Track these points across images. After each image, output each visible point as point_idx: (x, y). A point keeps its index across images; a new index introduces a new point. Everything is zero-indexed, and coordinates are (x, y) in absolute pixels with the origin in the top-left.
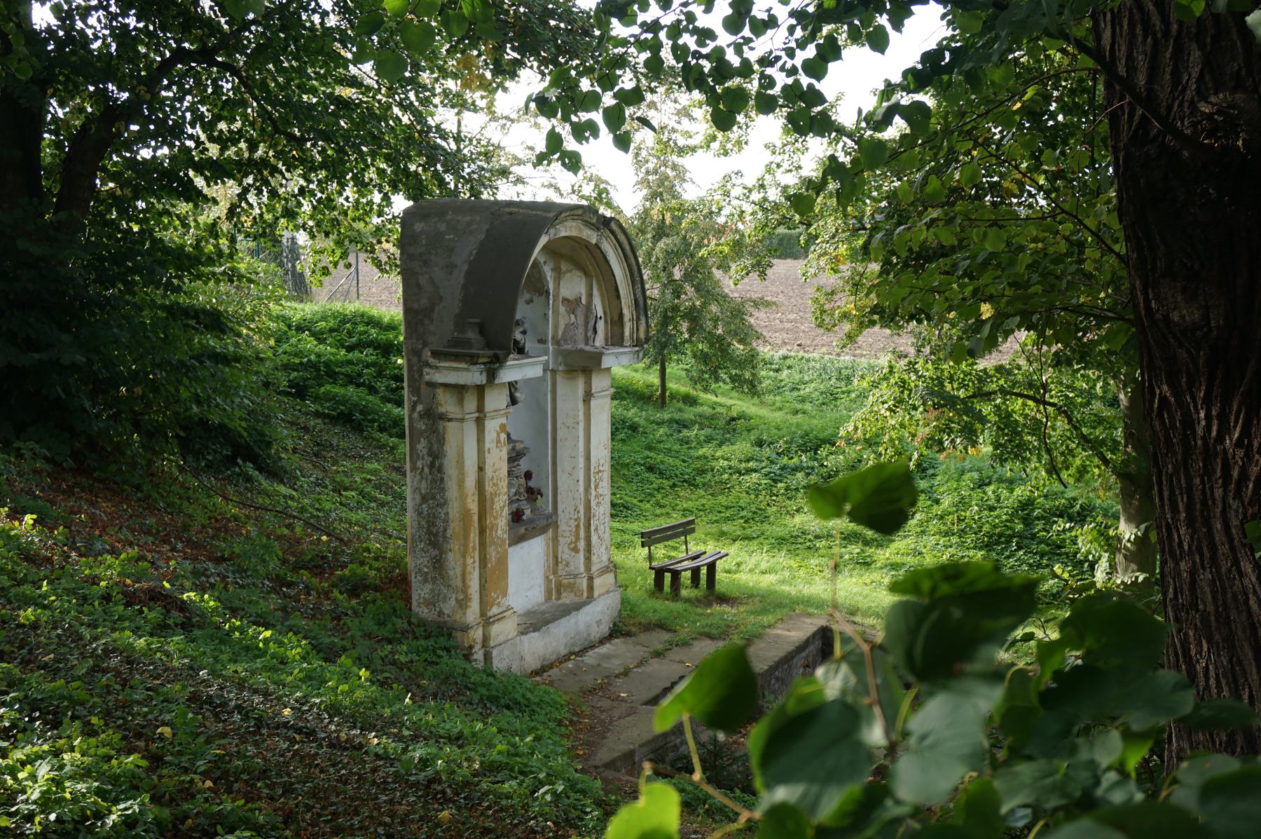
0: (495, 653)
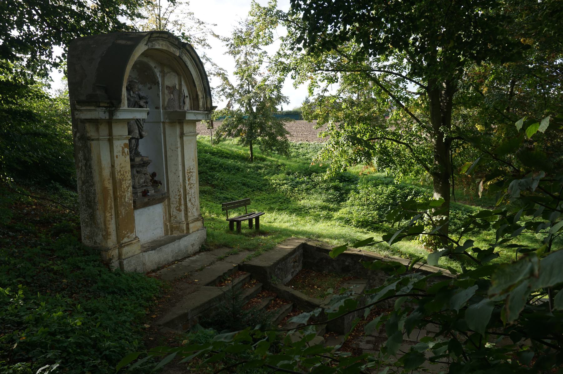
0: (125, 262)
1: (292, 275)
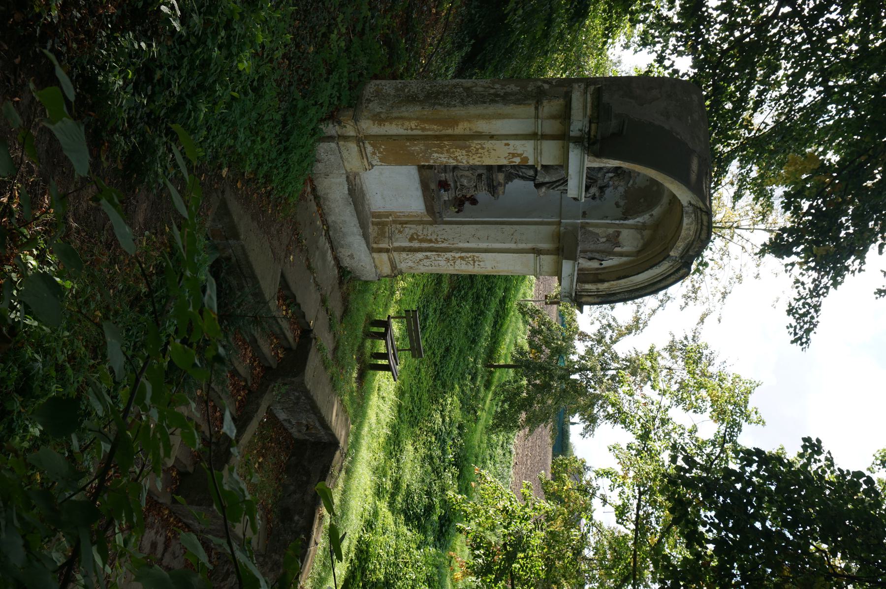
0: (333, 145)
1: (285, 420)
